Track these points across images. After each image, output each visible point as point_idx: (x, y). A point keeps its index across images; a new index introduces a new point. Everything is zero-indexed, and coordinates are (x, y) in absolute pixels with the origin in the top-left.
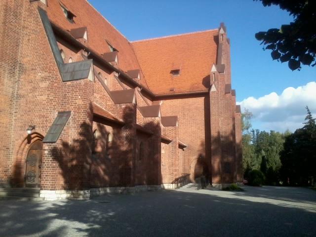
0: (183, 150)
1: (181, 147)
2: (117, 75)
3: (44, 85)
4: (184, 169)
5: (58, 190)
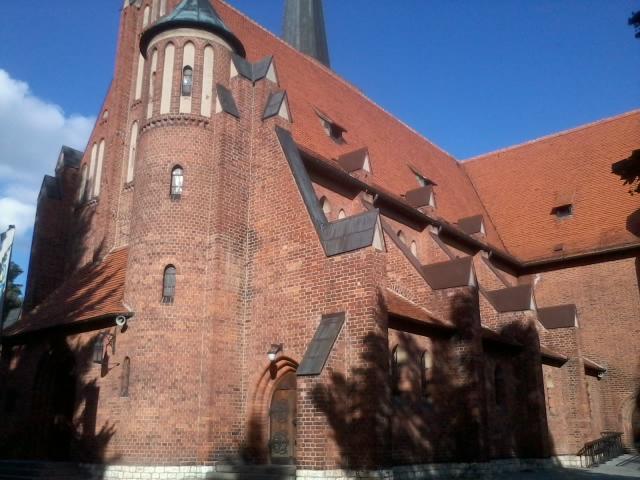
0: (599, 379)
1: (592, 371)
2: (435, 231)
4: (606, 421)
5: (330, 469)
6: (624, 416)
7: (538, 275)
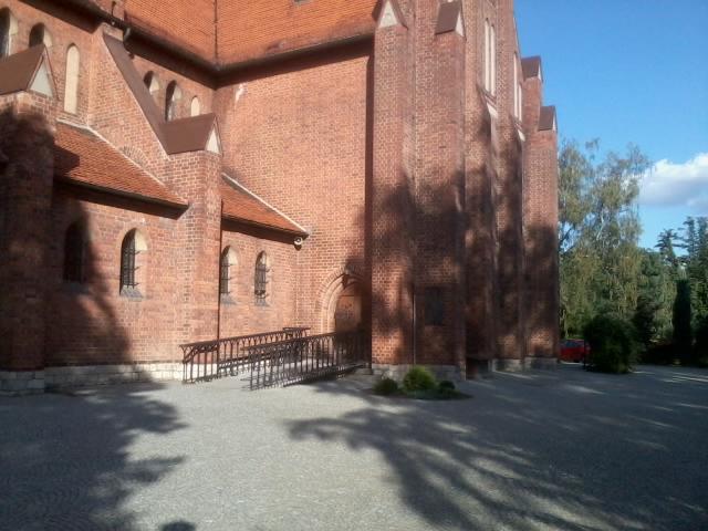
0: (298, 248)
6: (324, 304)
7: (241, 86)
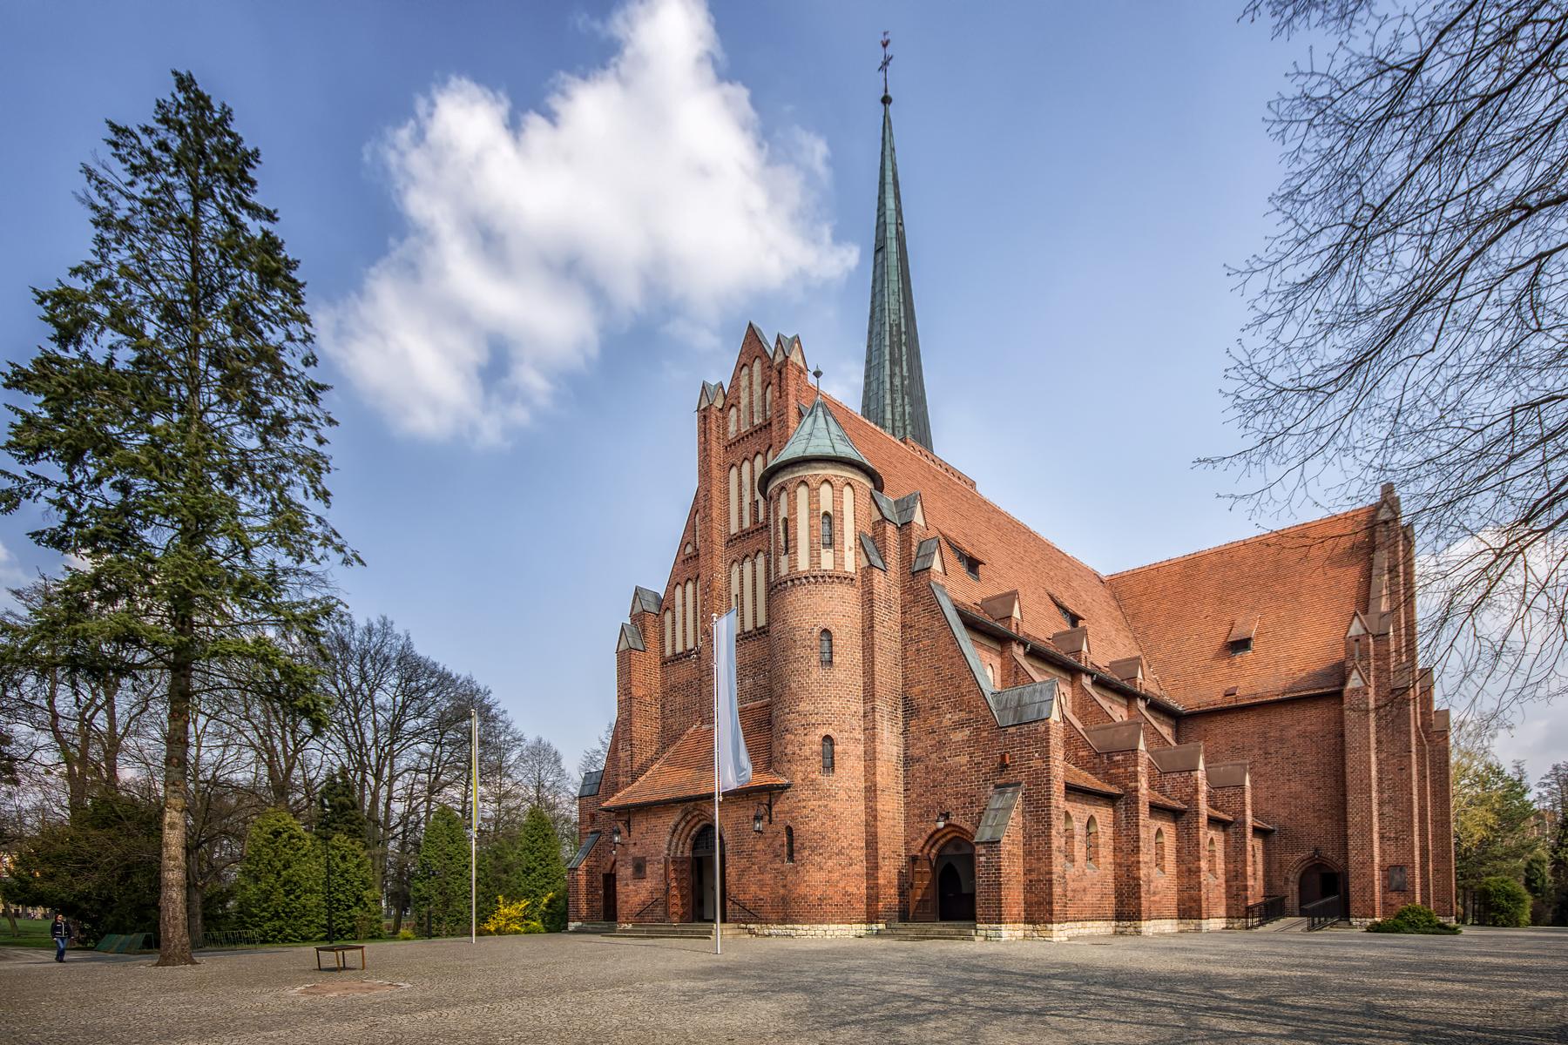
3: (959, 736)
